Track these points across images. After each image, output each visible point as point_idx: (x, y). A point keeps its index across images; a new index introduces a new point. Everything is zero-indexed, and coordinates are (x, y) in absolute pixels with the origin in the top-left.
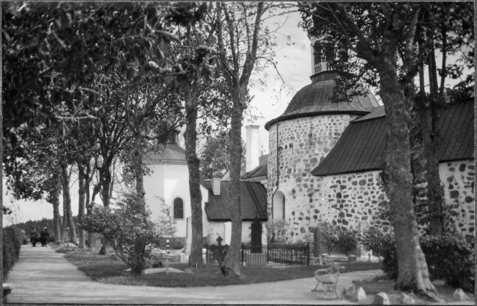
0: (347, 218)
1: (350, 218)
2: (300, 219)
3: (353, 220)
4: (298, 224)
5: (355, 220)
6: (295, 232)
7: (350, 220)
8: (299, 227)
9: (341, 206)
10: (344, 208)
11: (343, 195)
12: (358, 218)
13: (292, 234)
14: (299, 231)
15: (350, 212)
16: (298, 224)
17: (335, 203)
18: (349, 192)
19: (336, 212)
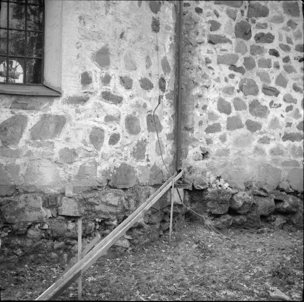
0: (264, 99)
1: (273, 98)
2: (126, 83)
3: (280, 105)
4: (118, 100)
5: (285, 105)
6: (108, 130)
7: (272, 103)
8: (124, 110)
9: (249, 64)
10: (258, 68)
11: (255, 32)
12: (295, 101)
13: (96, 137)
14: (120, 128)
15: (273, 84)
16: (118, 100)
17: (229, 48)
18: (275, 29)
19: (232, 76)
